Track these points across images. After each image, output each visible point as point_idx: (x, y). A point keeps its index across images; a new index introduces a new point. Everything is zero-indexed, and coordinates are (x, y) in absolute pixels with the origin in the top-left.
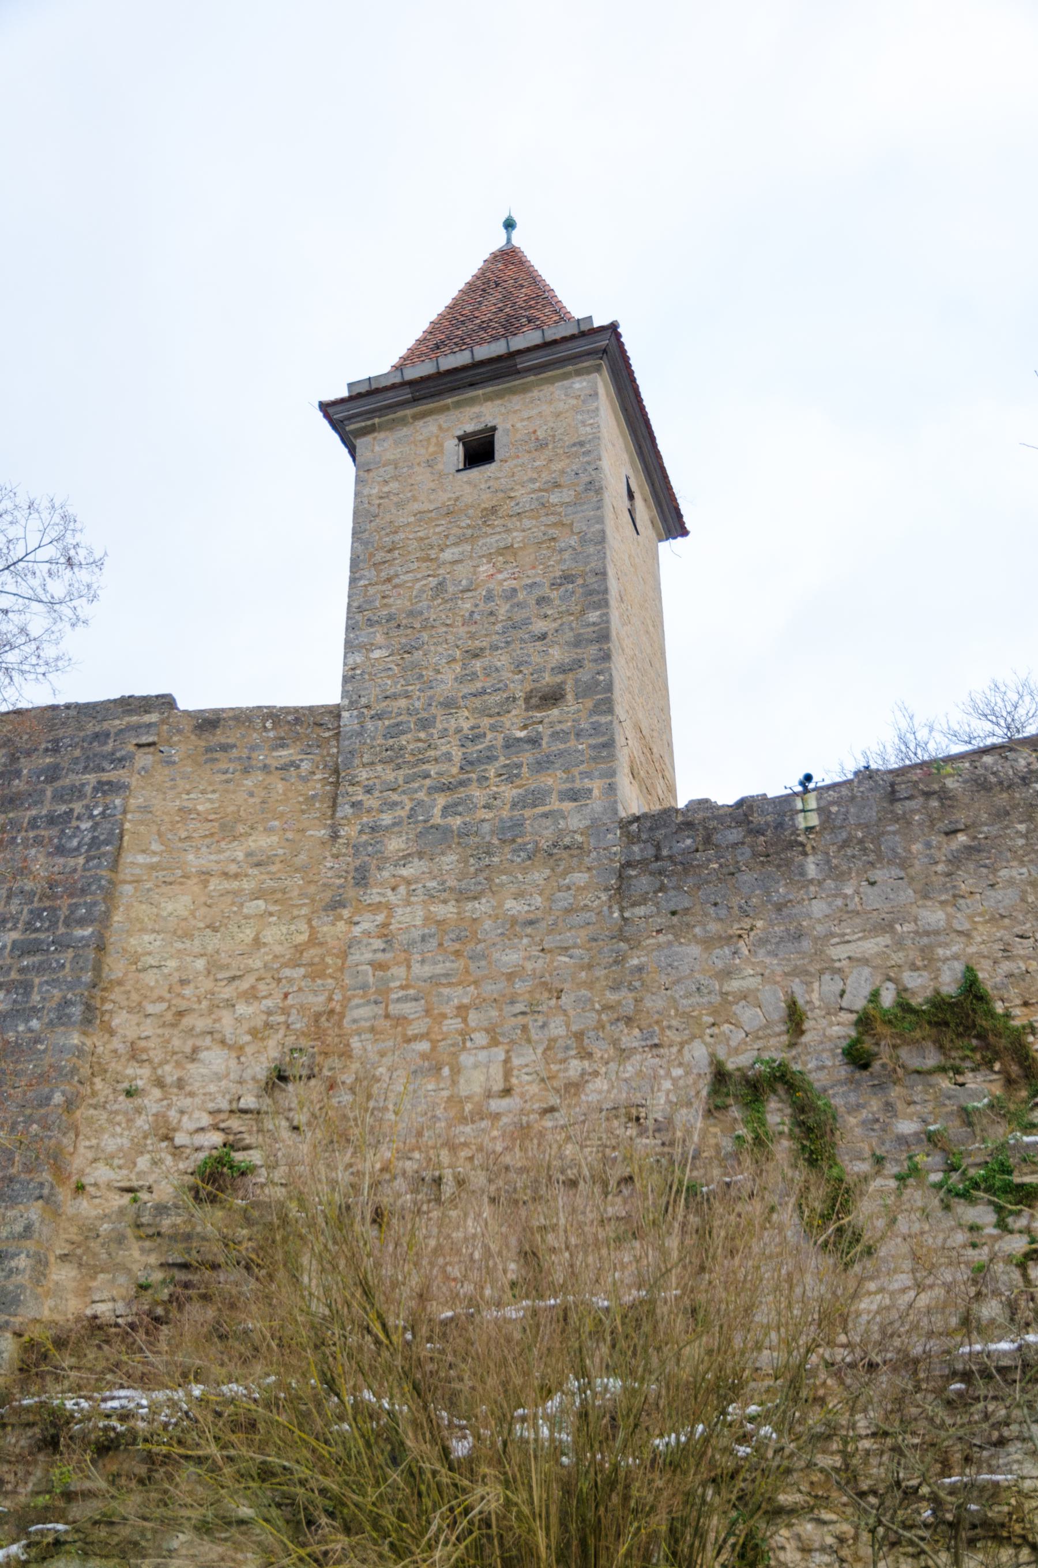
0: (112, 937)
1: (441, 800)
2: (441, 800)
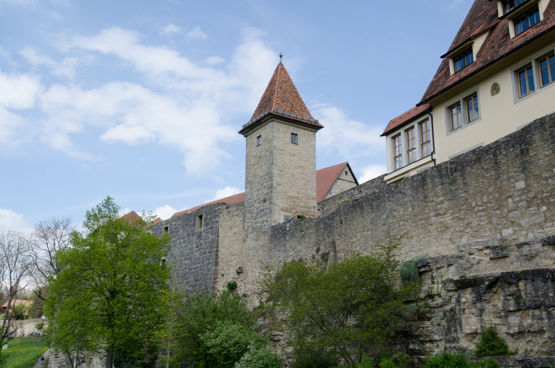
0: (219, 249)
1: (254, 221)
2: (254, 221)
